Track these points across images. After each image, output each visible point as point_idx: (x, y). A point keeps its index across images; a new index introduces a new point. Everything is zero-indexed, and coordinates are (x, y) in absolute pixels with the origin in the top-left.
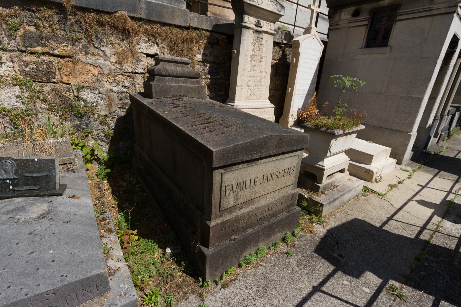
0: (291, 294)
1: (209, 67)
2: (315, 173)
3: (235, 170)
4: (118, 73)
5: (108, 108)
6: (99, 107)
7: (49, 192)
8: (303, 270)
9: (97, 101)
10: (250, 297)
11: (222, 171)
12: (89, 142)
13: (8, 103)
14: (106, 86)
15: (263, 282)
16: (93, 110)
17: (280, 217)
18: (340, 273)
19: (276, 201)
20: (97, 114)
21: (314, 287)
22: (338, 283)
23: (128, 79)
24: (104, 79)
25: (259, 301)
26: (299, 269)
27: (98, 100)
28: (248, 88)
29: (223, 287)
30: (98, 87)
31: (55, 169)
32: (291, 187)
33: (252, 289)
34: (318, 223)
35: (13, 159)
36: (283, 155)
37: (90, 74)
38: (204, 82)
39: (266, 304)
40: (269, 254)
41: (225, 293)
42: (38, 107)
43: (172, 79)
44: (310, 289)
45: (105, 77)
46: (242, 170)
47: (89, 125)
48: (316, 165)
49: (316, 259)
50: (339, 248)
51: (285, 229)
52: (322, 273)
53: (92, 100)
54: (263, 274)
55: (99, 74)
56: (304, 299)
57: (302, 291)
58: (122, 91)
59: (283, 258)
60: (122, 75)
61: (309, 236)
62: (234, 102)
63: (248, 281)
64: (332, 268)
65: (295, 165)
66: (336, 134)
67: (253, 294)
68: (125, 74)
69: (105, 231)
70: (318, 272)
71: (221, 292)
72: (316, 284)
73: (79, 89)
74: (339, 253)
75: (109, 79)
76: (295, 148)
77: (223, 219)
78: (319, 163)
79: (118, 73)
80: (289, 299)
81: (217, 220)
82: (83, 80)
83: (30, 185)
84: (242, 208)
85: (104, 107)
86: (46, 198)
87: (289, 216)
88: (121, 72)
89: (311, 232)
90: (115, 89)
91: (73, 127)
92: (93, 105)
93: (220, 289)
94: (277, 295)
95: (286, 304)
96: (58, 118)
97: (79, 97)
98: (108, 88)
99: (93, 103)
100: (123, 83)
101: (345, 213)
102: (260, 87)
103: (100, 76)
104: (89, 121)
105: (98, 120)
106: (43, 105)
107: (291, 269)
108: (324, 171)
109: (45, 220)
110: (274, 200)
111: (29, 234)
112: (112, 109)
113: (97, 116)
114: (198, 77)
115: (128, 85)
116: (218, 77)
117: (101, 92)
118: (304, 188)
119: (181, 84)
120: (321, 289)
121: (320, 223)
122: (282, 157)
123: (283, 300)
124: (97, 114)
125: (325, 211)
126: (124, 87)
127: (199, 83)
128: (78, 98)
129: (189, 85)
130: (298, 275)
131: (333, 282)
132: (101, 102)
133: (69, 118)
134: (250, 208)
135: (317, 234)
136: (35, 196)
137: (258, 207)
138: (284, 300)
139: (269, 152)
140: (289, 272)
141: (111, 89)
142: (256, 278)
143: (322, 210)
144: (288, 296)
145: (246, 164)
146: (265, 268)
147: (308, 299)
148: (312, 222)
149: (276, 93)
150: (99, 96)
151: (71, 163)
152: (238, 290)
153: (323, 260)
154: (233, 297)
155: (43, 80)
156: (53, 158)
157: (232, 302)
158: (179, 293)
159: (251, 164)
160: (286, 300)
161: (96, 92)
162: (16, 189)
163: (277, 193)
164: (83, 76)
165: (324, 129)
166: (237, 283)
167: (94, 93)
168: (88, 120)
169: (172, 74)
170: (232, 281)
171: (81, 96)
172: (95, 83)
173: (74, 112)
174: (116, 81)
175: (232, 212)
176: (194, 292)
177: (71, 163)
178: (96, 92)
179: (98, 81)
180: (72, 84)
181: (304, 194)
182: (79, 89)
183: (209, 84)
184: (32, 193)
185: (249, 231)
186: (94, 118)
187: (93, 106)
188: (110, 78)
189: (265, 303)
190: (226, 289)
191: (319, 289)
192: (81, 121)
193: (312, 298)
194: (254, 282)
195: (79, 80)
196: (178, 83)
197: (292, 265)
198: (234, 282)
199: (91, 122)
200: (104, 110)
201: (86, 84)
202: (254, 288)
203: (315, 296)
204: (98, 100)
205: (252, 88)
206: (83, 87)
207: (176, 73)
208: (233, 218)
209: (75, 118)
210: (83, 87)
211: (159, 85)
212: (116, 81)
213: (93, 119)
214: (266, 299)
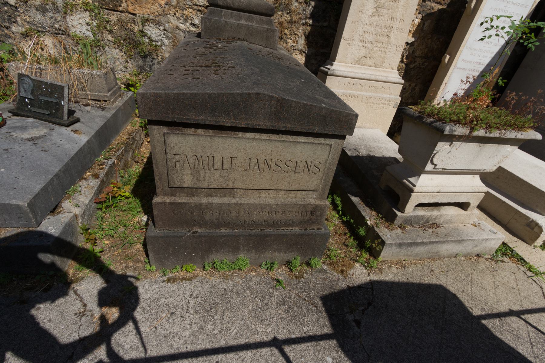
0: (235, 331)
1: (314, 7)
2: (399, 192)
3: (188, 134)
4: (188, 5)
6: (163, 48)
7: (58, 120)
8: (280, 312)
9: (162, 40)
10: (185, 306)
11: (165, 130)
13: (80, 30)
14: (172, 21)
15: (216, 299)
16: (157, 51)
17: (285, 230)
18: (333, 342)
19: (276, 205)
20: (161, 55)
21: (275, 339)
22: (317, 354)
23: (199, 15)
24: (171, 12)
25: (191, 316)
26: (277, 307)
27: (163, 39)
28: (361, 44)
29: (169, 281)
30: (164, 22)
31: (63, 96)
32: (314, 195)
33: (195, 299)
34: (364, 266)
35: (31, 79)
36: (294, 137)
37: (157, 4)
38: (300, 31)
39: (195, 323)
40: (256, 272)
41: (164, 289)
42: (105, 38)
43: (232, 13)
44: (269, 338)
45: (172, 10)
46: (201, 139)
47: (153, 68)
48: (405, 181)
49: (314, 308)
50: (366, 312)
51: (292, 251)
52: (305, 329)
53: (156, 38)
54: (225, 289)
55: (166, 4)
56: (247, 345)
57: (253, 335)
58: (190, 30)
59: (267, 285)
60: (192, 8)
61: (334, 274)
63: (200, 289)
64: (327, 330)
65: (322, 160)
66: (446, 132)
67: (192, 305)
68: (195, 7)
69: (92, 175)
70: (301, 325)
71: (162, 284)
72: (281, 337)
73: (145, 21)
74: (358, 318)
75: (176, 13)
76: (317, 130)
77: (175, 200)
78: (410, 179)
79: (188, 5)
80: (229, 334)
81: (166, 197)
82: (148, 11)
83: (43, 109)
84: (211, 195)
85: (169, 49)
86: (49, 124)
87: (302, 235)
88: (191, 4)
89: (342, 272)
90: (182, 26)
91: (137, 68)
92: (157, 44)
93: (163, 282)
94: (219, 321)
95: (219, 337)
96: (123, 54)
97: (144, 32)
98: (174, 24)
99: (157, 42)
100: (191, 20)
101: (429, 271)
102: (385, 45)
103: (167, 7)
104: (153, 63)
106: (110, 37)
107: (266, 302)
108: (413, 194)
109: (29, 143)
110: (273, 202)
111: (4, 150)
113: (161, 58)
114: (270, 13)
115: (198, 22)
116: (325, 24)
117: (166, 28)
118: (375, 211)
119: (242, 22)
120: (283, 347)
121: (367, 265)
122: (291, 140)
123: (219, 331)
124: (161, 55)
125: (386, 254)
126: (193, 25)
127: (270, 23)
128: (143, 33)
129: (254, 24)
130: (268, 314)
131: (311, 348)
132: (166, 41)
133: (134, 57)
134: (226, 200)
135: (350, 278)
136: (45, 121)
137: (239, 202)
138: (220, 332)
139: (255, 122)
140: (260, 304)
141: (178, 27)
142: (212, 290)
143: (381, 251)
144: (230, 330)
145: (211, 131)
146: (234, 285)
147: (252, 349)
148: (357, 261)
149: (426, 64)
150: (164, 34)
151: (106, 101)
152: (180, 292)
153: (324, 314)
154: (168, 297)
155: (110, 7)
156: (63, 85)
157: (163, 301)
158: (121, 264)
159: (222, 134)
160: (223, 333)
161: (161, 28)
162: (33, 109)
163: (281, 194)
164: (149, 6)
165: (430, 120)
166: (186, 284)
167: (159, 30)
168: (152, 61)
169: (232, 5)
170: (183, 279)
171: (146, 31)
172: (161, 17)
173: (139, 50)
174: (185, 16)
175: (194, 196)
176: (137, 270)
177: (106, 101)
178: (161, 28)
179: (165, 14)
180: (138, 15)
181: (368, 219)
182: (145, 21)
183: (309, 33)
184: (43, 117)
185: (223, 231)
186: (157, 60)
187: (156, 46)
188: (177, 11)
189: (196, 322)
190: (169, 284)
191: (281, 346)
192: (145, 61)
193: (259, 350)
194: (206, 293)
195: (144, 11)
196: (238, 20)
197: (272, 299)
198: (184, 282)
199: (154, 64)
201: (151, 17)
202: (199, 300)
203: (265, 351)
204: (163, 39)
205: (369, 45)
206: (147, 20)
207: (237, 4)
208: (191, 203)
209: (139, 57)
210: (147, 20)
211: (211, 19)
212: (185, 16)
213: (156, 61)
214: (201, 319)
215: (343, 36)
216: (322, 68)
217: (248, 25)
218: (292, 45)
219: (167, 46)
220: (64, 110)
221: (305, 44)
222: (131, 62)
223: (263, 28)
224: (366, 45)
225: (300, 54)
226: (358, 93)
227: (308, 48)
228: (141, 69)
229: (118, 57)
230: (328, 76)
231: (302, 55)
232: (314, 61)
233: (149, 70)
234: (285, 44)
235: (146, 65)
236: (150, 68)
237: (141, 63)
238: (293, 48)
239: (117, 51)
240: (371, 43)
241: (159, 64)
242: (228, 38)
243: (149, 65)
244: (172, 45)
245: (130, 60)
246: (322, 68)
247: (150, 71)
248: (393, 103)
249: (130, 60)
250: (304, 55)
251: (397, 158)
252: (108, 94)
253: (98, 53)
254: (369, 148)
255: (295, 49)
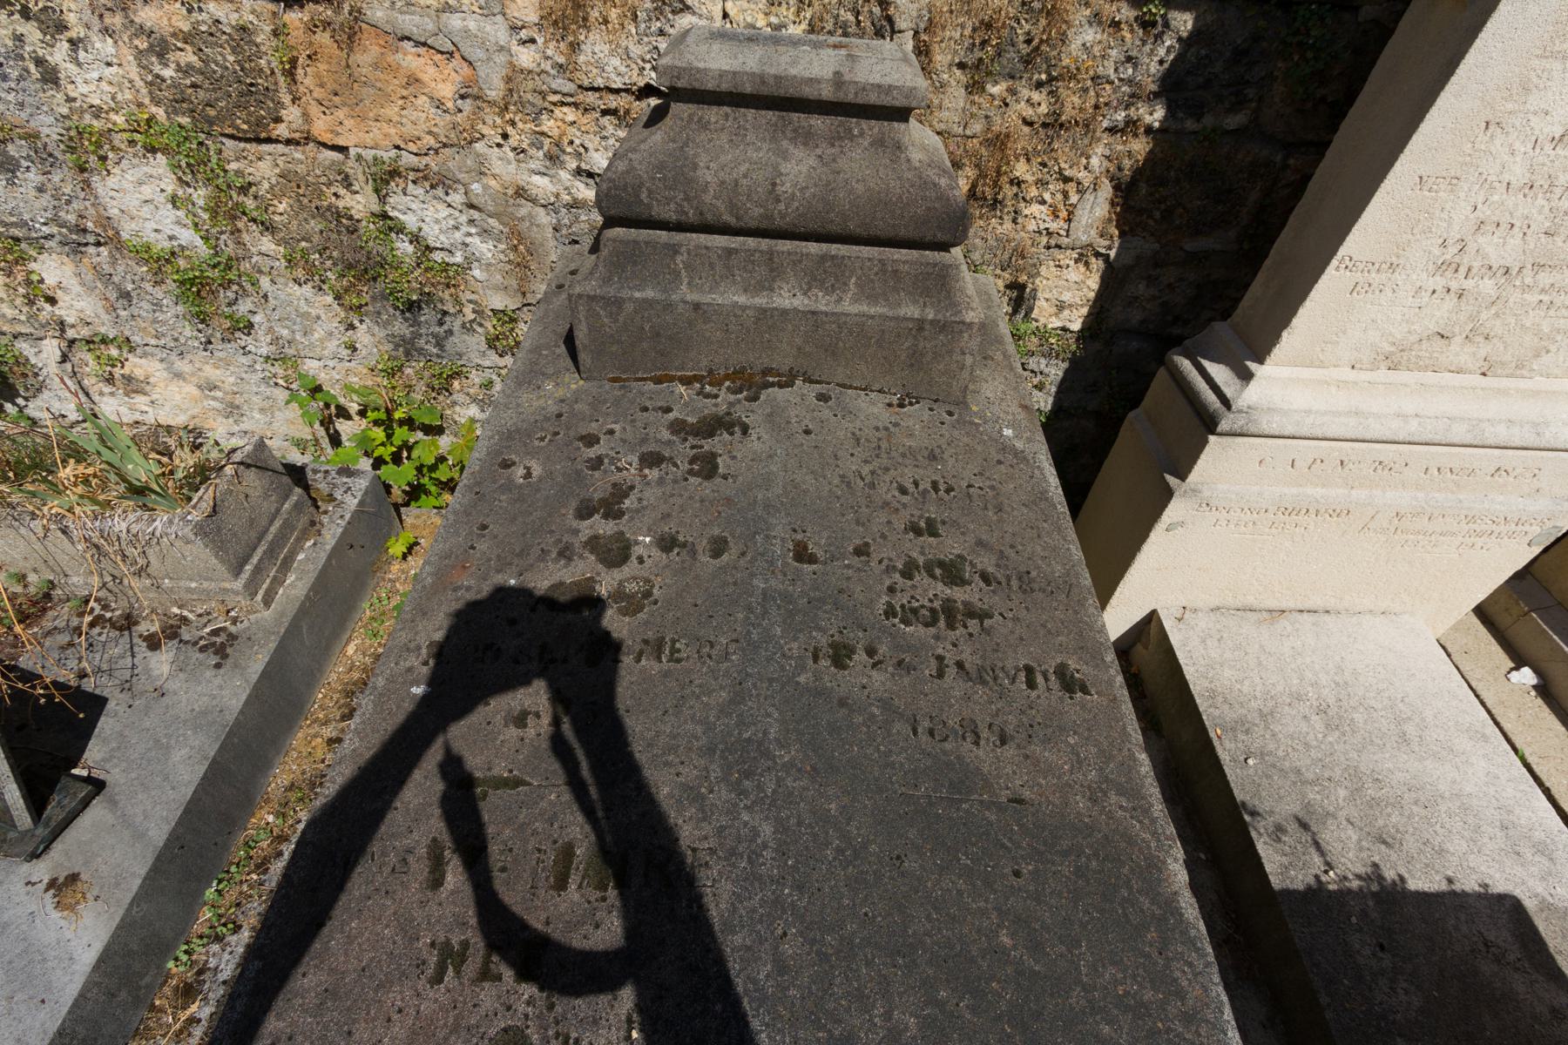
1: (1186, 43)
4: (555, 92)
5: (514, 283)
6: (477, 273)
12: (457, 408)
13: (155, 227)
14: (497, 167)
20: (470, 301)
23: (611, 129)
24: (486, 130)
27: (468, 240)
28: (1439, 282)
30: (460, 176)
37: (422, 100)
38: (1095, 161)
42: (254, 250)
47: (448, 347)
55: (462, 97)
58: (575, 199)
60: (576, 105)
62: (1246, 376)
68: (591, 98)
73: (385, 178)
75: (509, 129)
82: (393, 131)
85: (499, 277)
88: (569, 87)
90: (541, 185)
91: (391, 346)
96: (329, 299)
97: (391, 218)
98: (507, 178)
103: (467, 105)
104: (445, 327)
105: (480, 330)
106: (267, 244)
112: (533, 288)
113: (474, 311)
116: (1234, 121)
117: (475, 202)
119: (787, 298)
124: (470, 301)
127: (940, 284)
128: (388, 224)
132: (484, 248)
133: (370, 308)
150: (471, 222)
155: (238, 129)
161: (457, 198)
164: (391, 111)
168: (441, 323)
178: (457, 198)
180: (352, 152)
182: (385, 178)
183: (1138, 173)
188: (513, 123)
192: (416, 323)
199: (450, 332)
200: (497, 288)
201: (408, 159)
204: (468, 240)
205: (1488, 286)
206: (394, 173)
207: (757, 211)
209: (391, 310)
210: (394, 173)
211: (618, 303)
215: (1342, 251)
216: (1185, 365)
217: (813, 313)
218: (1042, 227)
219: (490, 265)
220: (10, 802)
221: (1110, 220)
222: (364, 326)
223: (897, 318)
224: (1469, 284)
225: (1076, 261)
226: (1360, 494)
227: (1122, 235)
228: (408, 348)
229: (314, 314)
230: (1212, 438)
231: (1087, 264)
232: (1142, 287)
233: (435, 351)
234: (1008, 225)
235: (421, 335)
236: (439, 344)
237: (401, 327)
238: (1044, 240)
239: (307, 290)
240: (1502, 271)
241: (468, 330)
242: (711, 372)
243: (435, 336)
244: (509, 262)
245: (361, 321)
246: (1185, 365)
247: (438, 356)
248: (1535, 530)
249: (361, 321)
250: (1097, 265)
251: (1530, 904)
252: (238, 584)
253: (240, 302)
254: (1374, 803)
255: (1059, 247)
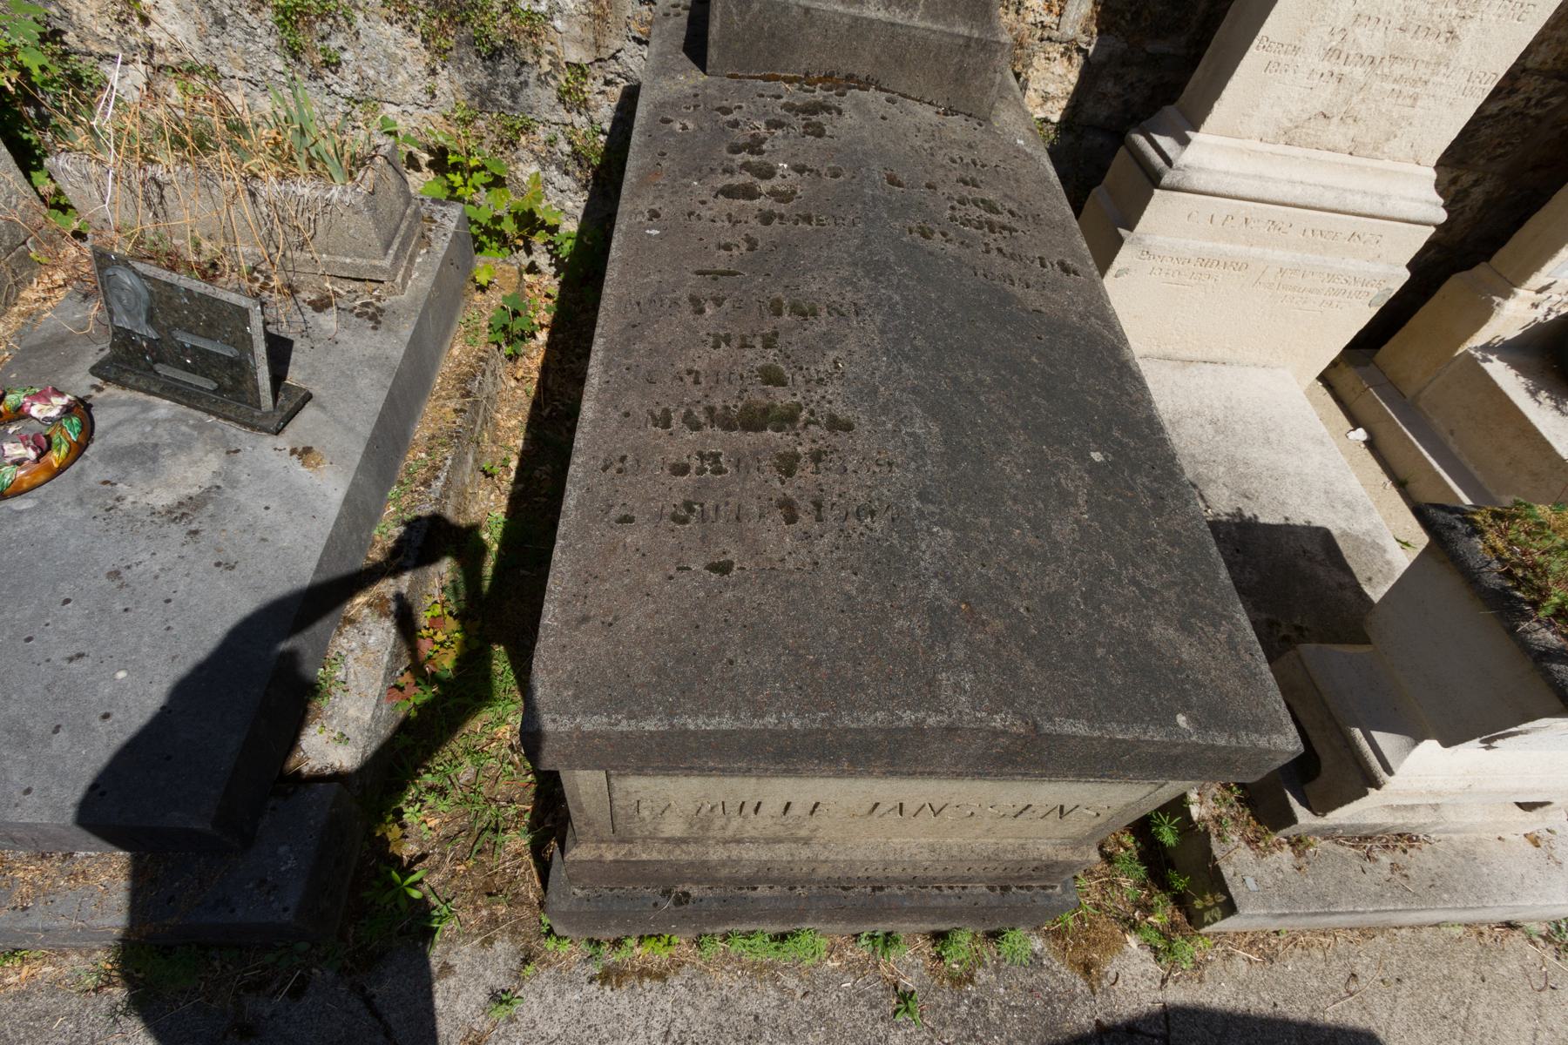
5: (590, 36)
6: (558, 23)
12: (521, 165)
16: (536, 35)
20: (549, 53)
28: (1325, 66)
34: (1155, 950)
47: (521, 99)
48: (1357, 732)
54: (756, 1018)
61: (1063, 975)
62: (1184, 142)
63: (688, 1011)
69: (369, 605)
77: (630, 853)
78: (1377, 735)
85: (578, 29)
89: (1087, 968)
91: (468, 95)
93: (591, 980)
96: (417, 41)
101: (1342, 976)
102: (1422, 70)
104: (522, 78)
105: (553, 83)
108: (1372, 791)
109: (177, 532)
112: (607, 43)
113: (551, 63)
121: (1163, 950)
133: (454, 53)
142: (722, 1018)
148: (1134, 927)
149: (1555, 101)
152: (637, 1021)
154: (606, 1035)
158: (476, 909)
166: (653, 994)
168: (518, 74)
170: (643, 973)
173: (471, 30)
190: (608, 988)
192: (494, 73)
194: (707, 1027)
198: (647, 982)
199: (525, 84)
200: (575, 40)
205: (1358, 73)
209: (473, 57)
213: (534, 75)
215: (1262, 32)
216: (1140, 140)
217: (893, 24)
218: (1038, 20)
219: (571, 16)
220: (260, 382)
221: (1091, 18)
222: (445, 73)
223: (952, 35)
224: (1346, 70)
225: (1062, 55)
226: (1256, 251)
227: (1100, 33)
228: (483, 98)
229: (400, 56)
230: (1157, 191)
231: (1070, 59)
232: (1110, 85)
233: (508, 102)
234: (1012, 15)
235: (497, 85)
236: (514, 97)
237: (480, 77)
238: (1039, 33)
239: (397, 30)
240: (1369, 60)
241: (542, 82)
242: (807, 75)
243: (511, 87)
244: (588, 15)
245: (443, 67)
246: (1140, 140)
247: (511, 108)
248: (1374, 291)
249: (443, 67)
250: (1078, 59)
251: (1335, 532)
252: (386, 263)
253: (332, 37)
254: (1242, 476)
255: (1049, 39)
